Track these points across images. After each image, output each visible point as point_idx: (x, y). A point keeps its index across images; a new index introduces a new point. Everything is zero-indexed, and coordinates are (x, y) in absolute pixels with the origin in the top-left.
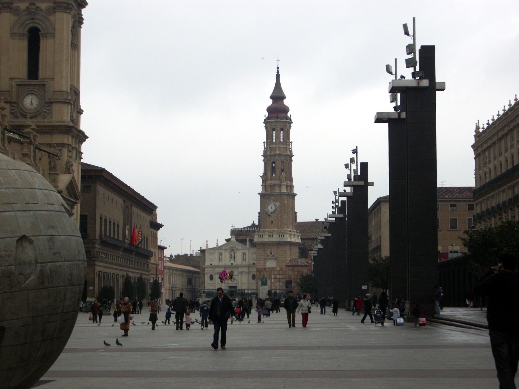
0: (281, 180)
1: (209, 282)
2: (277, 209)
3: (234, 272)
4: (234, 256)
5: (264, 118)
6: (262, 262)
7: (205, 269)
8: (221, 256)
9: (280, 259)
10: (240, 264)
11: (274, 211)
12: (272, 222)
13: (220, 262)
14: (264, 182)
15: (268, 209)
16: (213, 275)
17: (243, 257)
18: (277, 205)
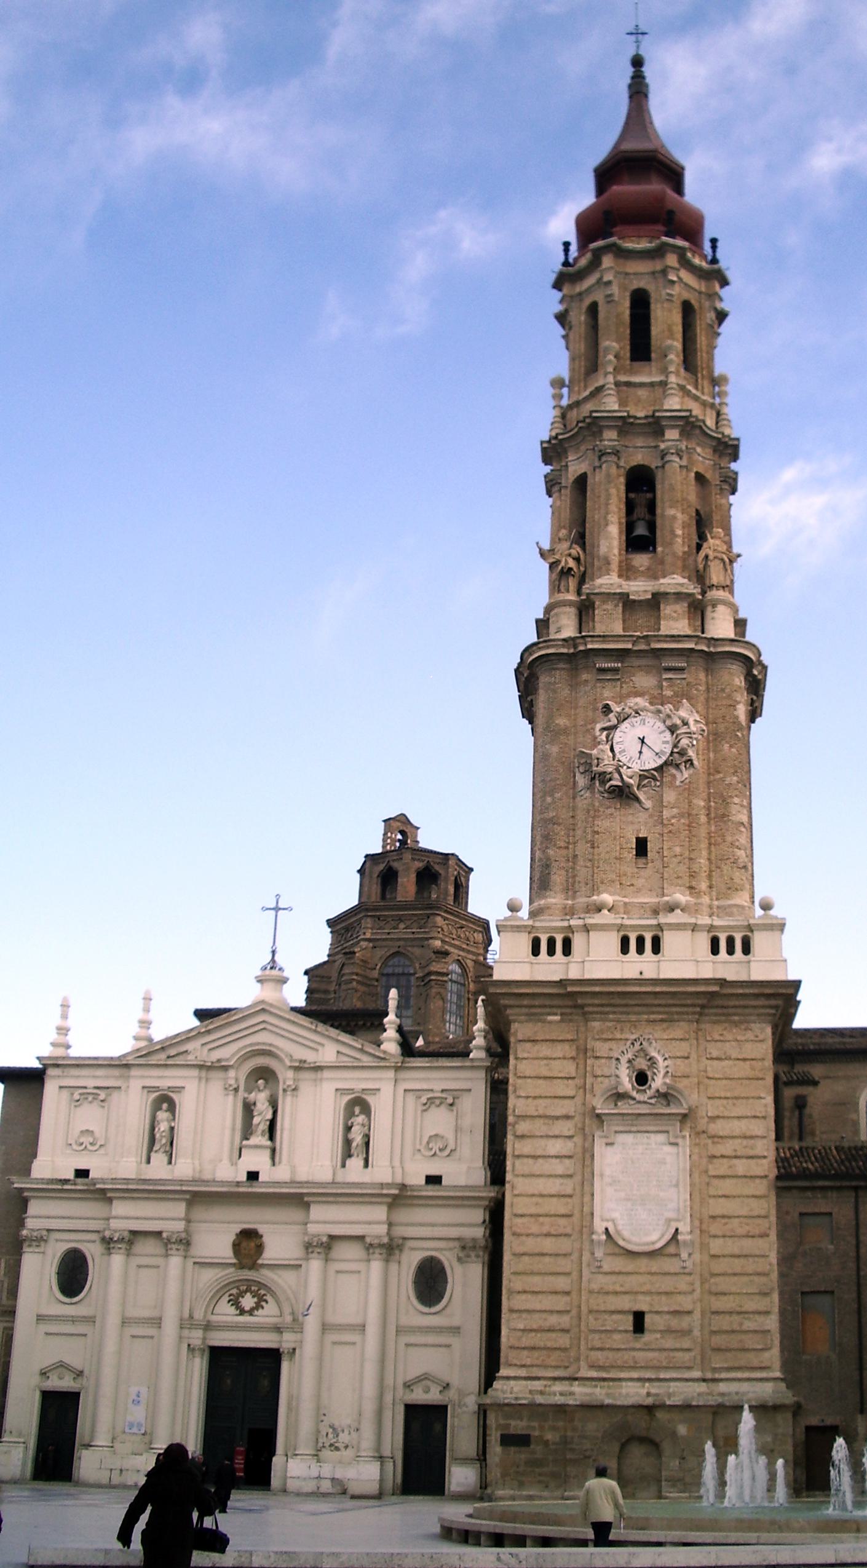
0: (700, 577)
1: (58, 1305)
2: (691, 753)
3: (266, 1239)
4: (269, 1116)
5: (562, 258)
6: (556, 1147)
7: (25, 1202)
8: (162, 1115)
9: (718, 1127)
10: (325, 1176)
11: (660, 769)
12: (642, 847)
13: (158, 1158)
14: (572, 583)
15: (617, 749)
16: (92, 1250)
17: (348, 1129)
18: (691, 722)
